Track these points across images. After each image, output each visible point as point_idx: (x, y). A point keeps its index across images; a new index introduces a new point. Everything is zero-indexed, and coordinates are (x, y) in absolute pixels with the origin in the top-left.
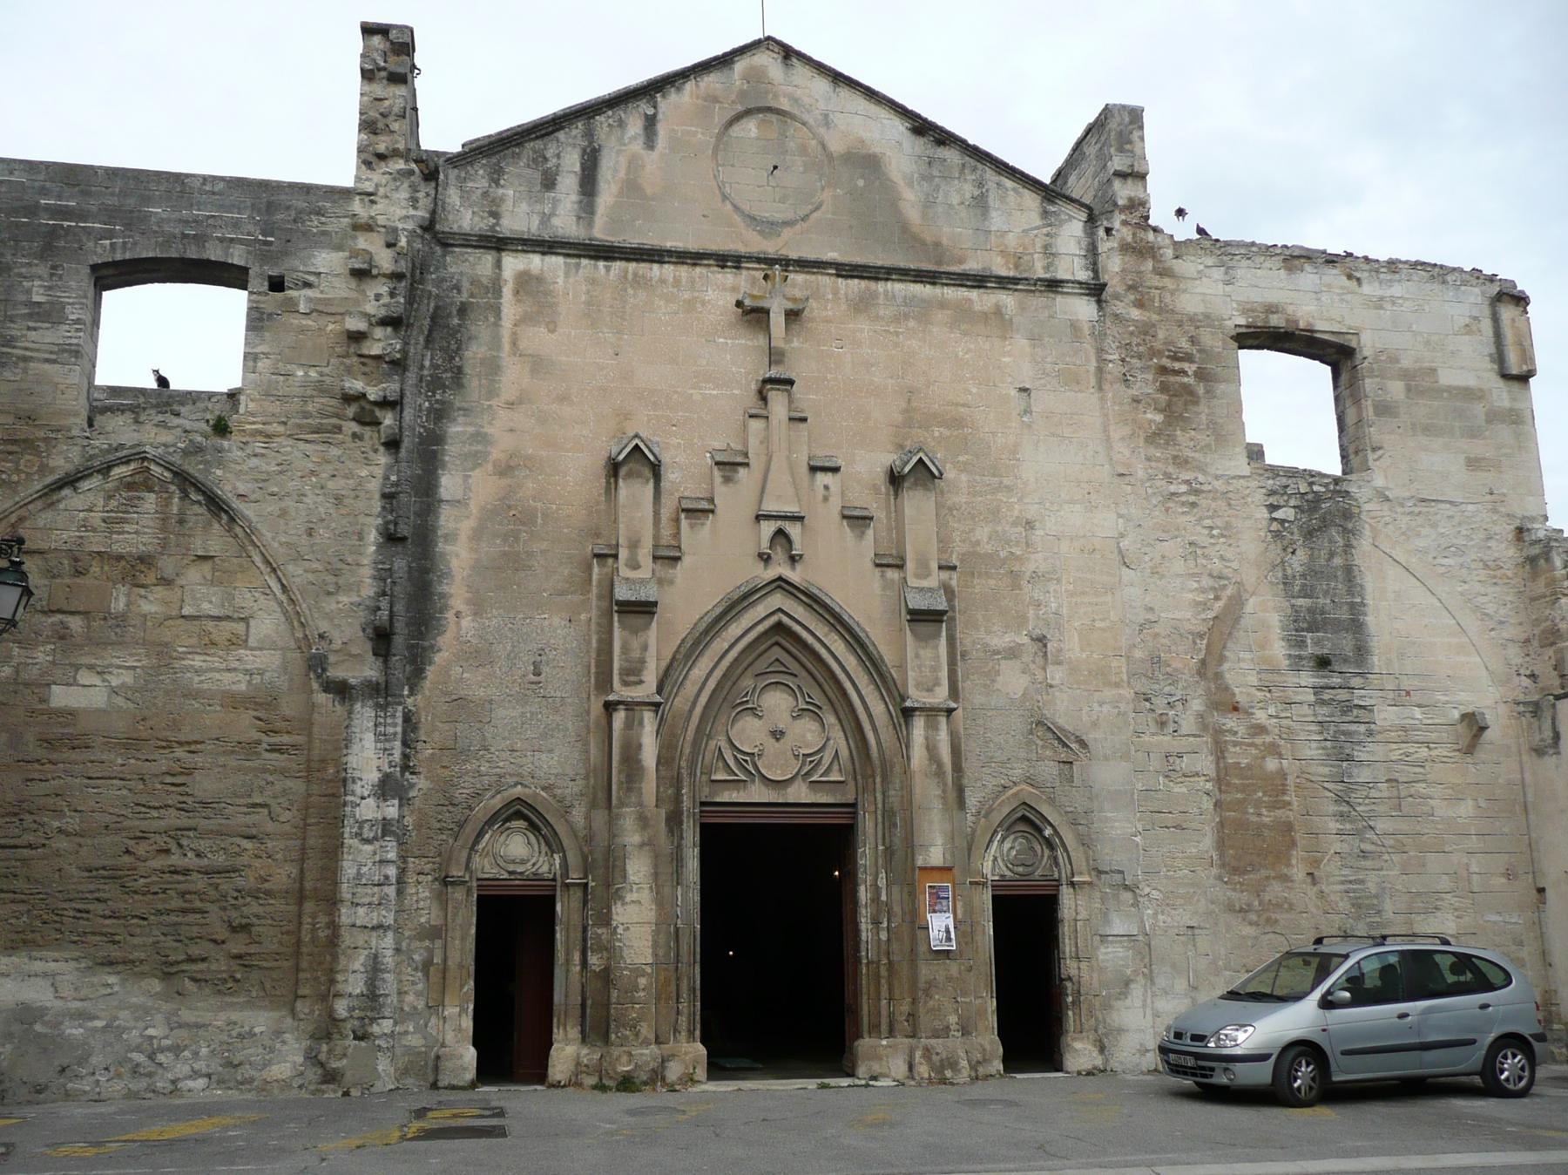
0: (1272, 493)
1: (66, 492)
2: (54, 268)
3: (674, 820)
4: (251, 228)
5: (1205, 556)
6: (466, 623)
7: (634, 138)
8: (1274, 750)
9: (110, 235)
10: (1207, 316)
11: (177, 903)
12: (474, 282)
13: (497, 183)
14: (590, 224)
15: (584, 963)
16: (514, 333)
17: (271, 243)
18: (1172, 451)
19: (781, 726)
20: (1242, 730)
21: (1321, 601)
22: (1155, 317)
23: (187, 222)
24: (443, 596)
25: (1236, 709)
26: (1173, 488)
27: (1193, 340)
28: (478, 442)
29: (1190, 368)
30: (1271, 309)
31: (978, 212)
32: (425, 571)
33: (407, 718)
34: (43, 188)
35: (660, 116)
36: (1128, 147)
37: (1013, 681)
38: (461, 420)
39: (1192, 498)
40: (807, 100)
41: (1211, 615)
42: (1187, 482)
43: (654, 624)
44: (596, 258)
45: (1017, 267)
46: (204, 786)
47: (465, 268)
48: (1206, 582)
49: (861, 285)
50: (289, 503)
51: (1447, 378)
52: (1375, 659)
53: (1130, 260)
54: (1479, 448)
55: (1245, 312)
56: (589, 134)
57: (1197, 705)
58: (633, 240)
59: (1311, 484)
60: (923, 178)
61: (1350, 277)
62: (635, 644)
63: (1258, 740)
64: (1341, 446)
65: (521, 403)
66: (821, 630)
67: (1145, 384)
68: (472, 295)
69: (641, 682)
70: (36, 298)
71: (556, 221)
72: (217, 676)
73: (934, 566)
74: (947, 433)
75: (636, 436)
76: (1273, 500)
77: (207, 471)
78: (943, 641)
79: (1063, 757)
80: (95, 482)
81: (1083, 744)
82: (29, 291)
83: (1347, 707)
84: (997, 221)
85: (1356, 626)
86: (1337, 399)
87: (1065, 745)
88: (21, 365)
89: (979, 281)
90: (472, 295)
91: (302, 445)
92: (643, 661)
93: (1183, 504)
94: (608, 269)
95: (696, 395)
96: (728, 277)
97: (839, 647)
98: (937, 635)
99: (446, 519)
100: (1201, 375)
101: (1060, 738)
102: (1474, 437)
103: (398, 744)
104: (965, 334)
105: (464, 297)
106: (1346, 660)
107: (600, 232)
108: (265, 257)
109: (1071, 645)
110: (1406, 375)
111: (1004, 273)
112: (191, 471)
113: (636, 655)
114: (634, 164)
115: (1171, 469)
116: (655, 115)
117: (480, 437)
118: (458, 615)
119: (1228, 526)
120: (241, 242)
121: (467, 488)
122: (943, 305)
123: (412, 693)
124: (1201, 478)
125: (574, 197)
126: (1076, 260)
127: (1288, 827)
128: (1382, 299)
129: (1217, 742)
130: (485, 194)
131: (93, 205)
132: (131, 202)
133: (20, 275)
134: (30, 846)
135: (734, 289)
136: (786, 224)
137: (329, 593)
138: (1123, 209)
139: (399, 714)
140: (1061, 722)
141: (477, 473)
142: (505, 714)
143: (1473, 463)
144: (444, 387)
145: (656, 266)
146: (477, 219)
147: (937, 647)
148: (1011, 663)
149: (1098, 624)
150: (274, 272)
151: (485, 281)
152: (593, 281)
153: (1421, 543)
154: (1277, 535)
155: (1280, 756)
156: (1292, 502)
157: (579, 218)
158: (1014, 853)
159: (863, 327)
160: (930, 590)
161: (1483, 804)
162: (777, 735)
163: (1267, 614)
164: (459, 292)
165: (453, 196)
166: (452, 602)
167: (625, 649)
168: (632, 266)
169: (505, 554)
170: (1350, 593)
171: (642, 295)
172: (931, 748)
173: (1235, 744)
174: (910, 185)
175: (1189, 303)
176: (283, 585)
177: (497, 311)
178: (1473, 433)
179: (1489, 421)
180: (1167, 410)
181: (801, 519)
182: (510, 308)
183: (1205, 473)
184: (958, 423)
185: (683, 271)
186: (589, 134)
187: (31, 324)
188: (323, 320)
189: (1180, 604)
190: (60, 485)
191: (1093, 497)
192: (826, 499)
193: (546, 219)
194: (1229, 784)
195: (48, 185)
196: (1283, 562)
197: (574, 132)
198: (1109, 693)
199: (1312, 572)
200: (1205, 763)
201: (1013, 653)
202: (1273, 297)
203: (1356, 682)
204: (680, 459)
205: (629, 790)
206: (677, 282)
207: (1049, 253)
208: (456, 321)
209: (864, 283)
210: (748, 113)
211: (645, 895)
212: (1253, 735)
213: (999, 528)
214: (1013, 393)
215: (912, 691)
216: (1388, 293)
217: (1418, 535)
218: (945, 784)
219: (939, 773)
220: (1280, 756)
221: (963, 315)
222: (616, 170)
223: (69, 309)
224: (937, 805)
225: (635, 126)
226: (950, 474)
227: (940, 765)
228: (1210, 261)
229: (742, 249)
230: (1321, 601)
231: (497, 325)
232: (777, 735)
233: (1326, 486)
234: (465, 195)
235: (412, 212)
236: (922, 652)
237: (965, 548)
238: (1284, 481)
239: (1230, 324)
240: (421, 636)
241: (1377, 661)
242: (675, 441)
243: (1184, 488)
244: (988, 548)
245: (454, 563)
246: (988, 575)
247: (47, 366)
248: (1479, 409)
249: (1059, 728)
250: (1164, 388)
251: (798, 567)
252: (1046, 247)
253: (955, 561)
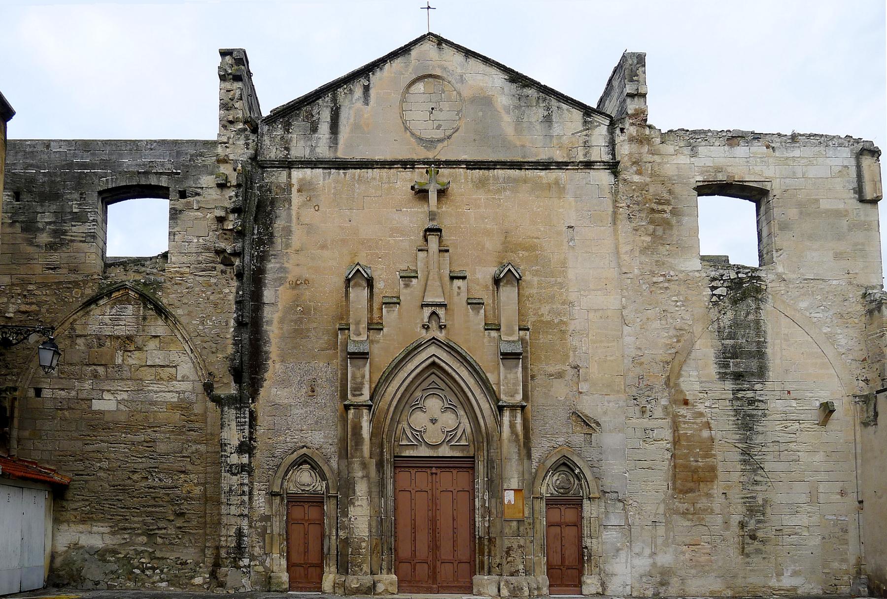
0: (714, 279)
1: (93, 306)
3: (380, 465)
5: (673, 318)
6: (277, 366)
11: (152, 502)
13: (288, 132)
14: (336, 150)
15: (337, 535)
18: (656, 257)
19: (435, 416)
20: (689, 415)
24: (266, 353)
26: (655, 279)
27: (670, 192)
28: (282, 272)
29: (668, 208)
32: (258, 340)
33: (251, 413)
35: (371, 86)
38: (273, 261)
39: (666, 285)
41: (673, 351)
42: (664, 275)
43: (368, 364)
46: (162, 447)
48: (672, 332)
49: (477, 173)
51: (825, 205)
52: (771, 373)
55: (701, 173)
59: (737, 273)
63: (698, 421)
65: (302, 250)
66: (456, 365)
69: (362, 394)
71: (318, 150)
72: (164, 394)
74: (527, 254)
75: (358, 264)
76: (714, 284)
77: (155, 293)
78: (520, 369)
79: (586, 431)
81: (598, 424)
83: (751, 402)
85: (760, 354)
87: (587, 425)
89: (546, 165)
91: (198, 278)
92: (362, 383)
93: (661, 288)
97: (464, 373)
98: (517, 366)
99: (267, 313)
102: (839, 239)
103: (247, 427)
106: (752, 374)
107: (342, 154)
109: (594, 371)
113: (359, 380)
115: (655, 268)
117: (283, 269)
119: (686, 299)
121: (277, 297)
123: (253, 402)
125: (328, 136)
130: (282, 138)
134: (88, 475)
135: (411, 180)
137: (213, 353)
139: (247, 412)
140: (587, 412)
141: (281, 288)
142: (298, 411)
144: (264, 244)
146: (278, 152)
147: (516, 373)
154: (715, 304)
158: (558, 482)
159: (481, 196)
160: (514, 342)
162: (434, 421)
163: (706, 352)
165: (267, 140)
166: (271, 355)
167: (354, 377)
169: (295, 330)
172: (512, 426)
173: (685, 423)
175: (669, 170)
180: (653, 234)
181: (445, 306)
182: (296, 198)
184: (531, 248)
186: (334, 100)
192: (459, 294)
193: (313, 149)
196: (718, 319)
197: (327, 99)
200: (668, 434)
201: (560, 375)
205: (356, 449)
206: (381, 178)
207: (587, 145)
209: (481, 172)
211: (365, 503)
212: (695, 418)
213: (555, 307)
215: (503, 397)
218: (520, 446)
219: (517, 439)
222: (348, 119)
224: (515, 457)
225: (358, 91)
226: (527, 277)
227: (517, 436)
229: (415, 157)
232: (434, 421)
233: (746, 273)
234: (272, 139)
236: (508, 376)
239: (693, 181)
240: (257, 373)
241: (771, 374)
243: (661, 279)
245: (271, 336)
248: (844, 223)
249: (586, 416)
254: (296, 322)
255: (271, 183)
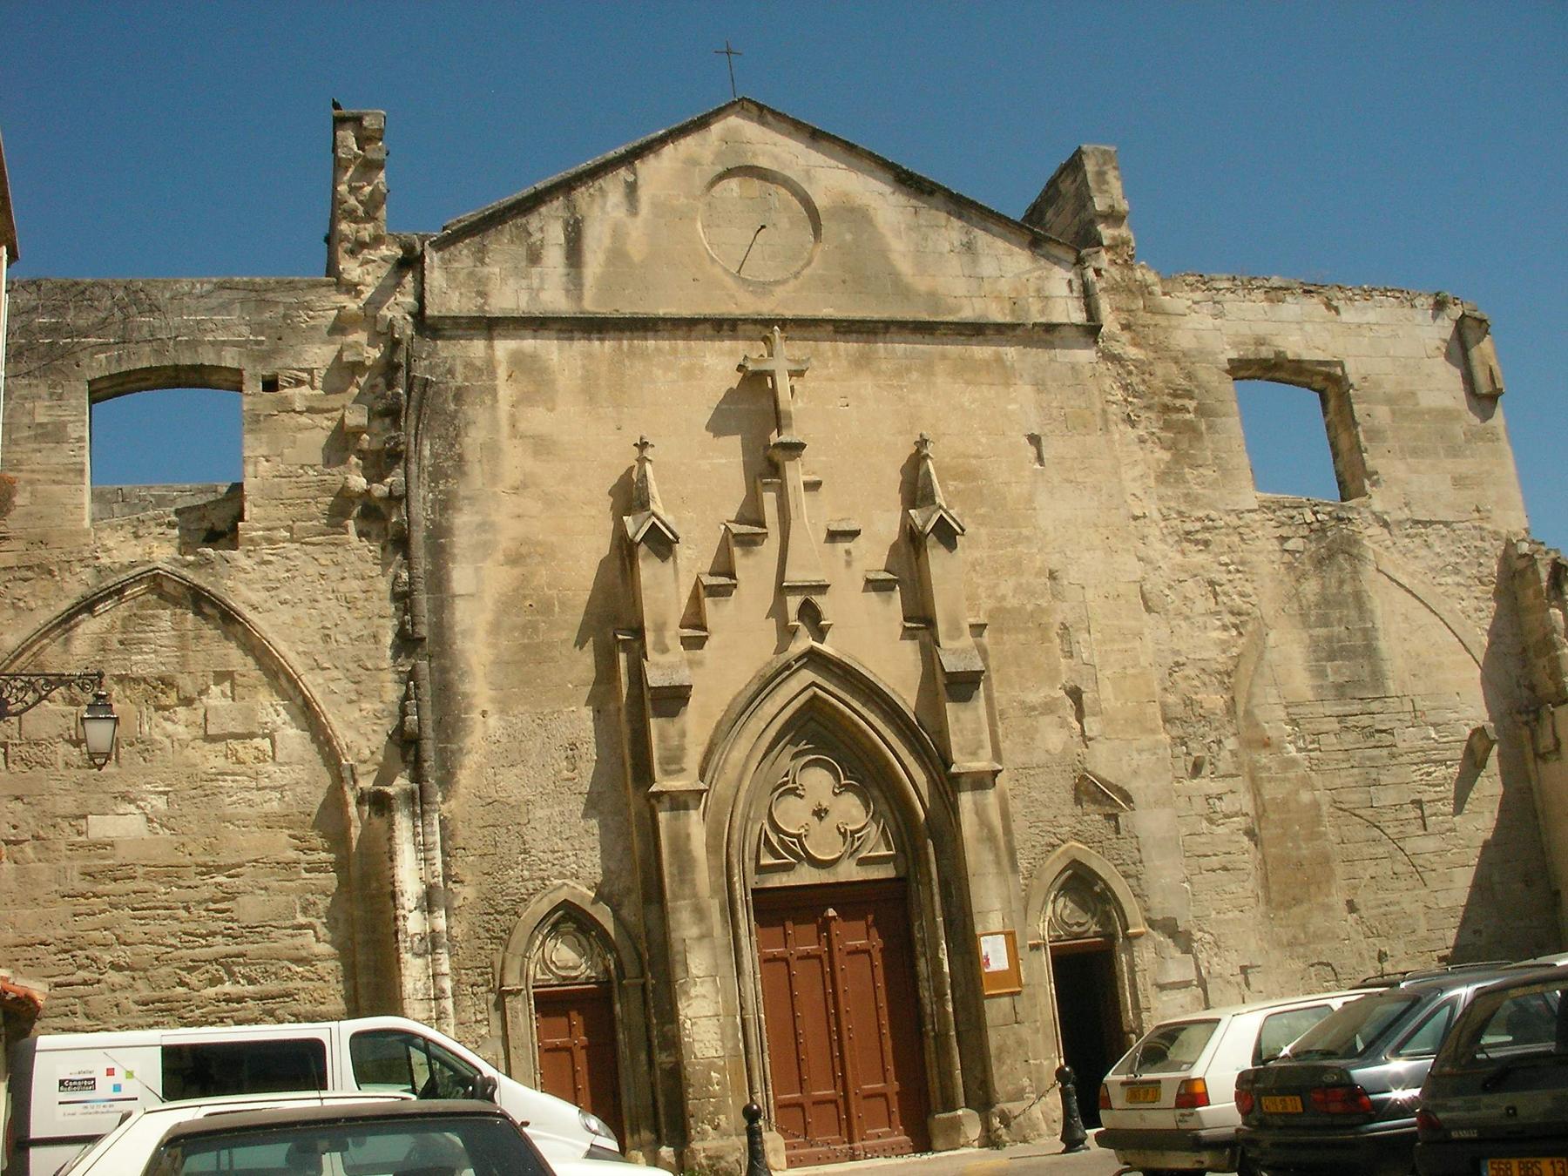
12: (469, 365)
13: (483, 263)
16: (512, 415)
22: (1152, 355)
29: (1191, 404)
38: (466, 509)
42: (1199, 519)
45: (1013, 311)
58: (627, 310)
67: (1150, 423)
90: (466, 379)
104: (968, 383)
105: (459, 380)
107: (592, 304)
111: (1000, 319)
124: (1213, 514)
130: (471, 274)
136: (777, 283)
144: (447, 476)
146: (464, 300)
151: (478, 363)
152: (589, 356)
159: (865, 384)
165: (435, 277)
169: (525, 647)
174: (898, 235)
177: (493, 391)
182: (506, 392)
183: (1216, 510)
198: (1145, 740)
208: (452, 407)
221: (965, 369)
231: (494, 407)
244: (1012, 602)
252: (1038, 290)
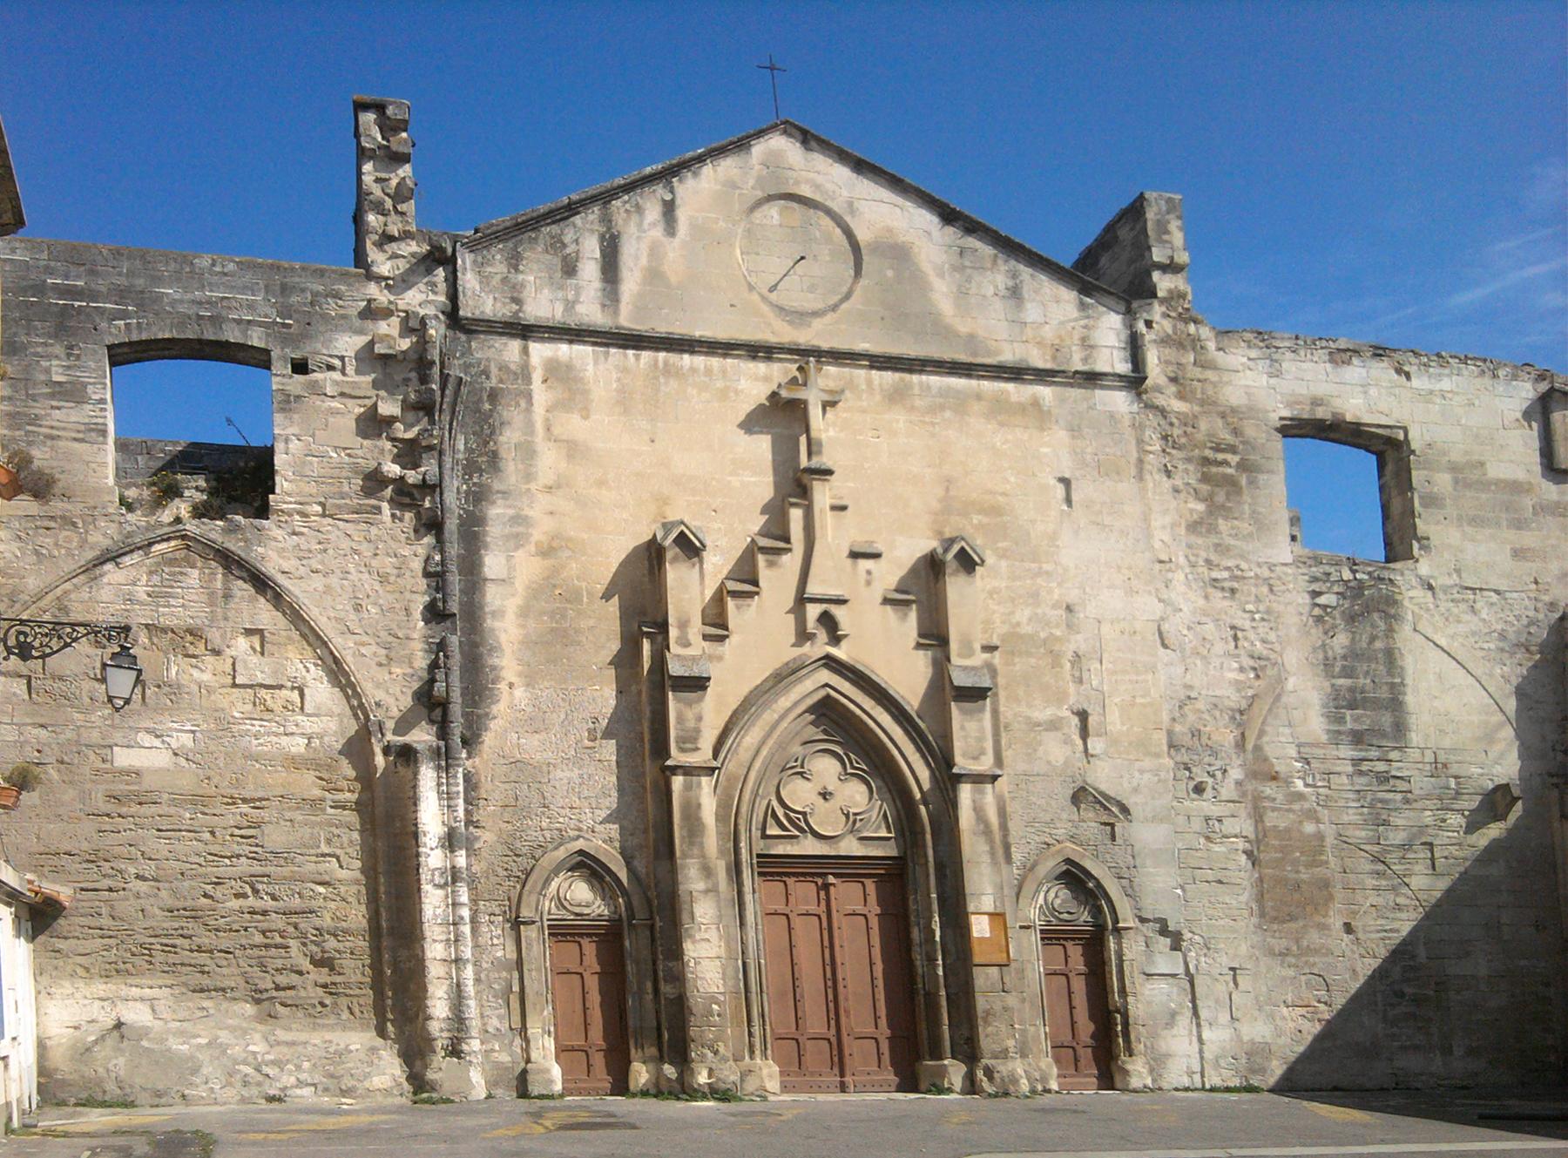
0: (1315, 579)
1: (109, 566)
2: (71, 347)
4: (269, 310)
6: (519, 692)
7: (654, 225)
8: (1312, 815)
9: (124, 315)
10: (1251, 409)
12: (503, 368)
13: (517, 270)
14: (616, 312)
15: (656, 990)
16: (547, 420)
17: (289, 326)
19: (830, 788)
20: (1280, 797)
21: (1362, 681)
22: (1197, 408)
23: (200, 303)
24: (494, 668)
25: (1274, 778)
26: (1215, 574)
27: (1236, 432)
29: (1233, 459)
30: (1316, 402)
31: (1012, 302)
32: (475, 645)
34: (47, 267)
35: (678, 202)
36: (1165, 237)
37: (1058, 751)
38: (499, 502)
40: (829, 186)
41: (1250, 693)
42: (1228, 569)
44: (625, 347)
45: (1054, 358)
47: (490, 353)
50: (334, 581)
51: (1496, 471)
52: (1413, 735)
53: (1171, 353)
54: (1529, 539)
55: (1289, 405)
56: (606, 220)
57: (1236, 774)
58: (662, 328)
60: (954, 268)
61: (1399, 371)
62: (690, 714)
63: (1296, 807)
64: (1385, 534)
65: (559, 487)
66: (868, 703)
67: (1188, 475)
68: (501, 381)
69: (697, 749)
70: (56, 378)
71: (581, 309)
73: (977, 646)
74: (985, 520)
76: (1316, 587)
77: (248, 548)
78: (987, 715)
79: (1105, 819)
80: (136, 557)
81: (1125, 810)
82: (48, 371)
83: (1383, 778)
84: (1032, 312)
85: (1395, 704)
86: (1381, 489)
87: (1106, 808)
88: (49, 443)
89: (1016, 373)
90: (501, 381)
94: (637, 358)
95: (735, 482)
96: (761, 367)
97: (885, 719)
98: (982, 710)
99: (493, 596)
100: (1243, 466)
101: (1102, 802)
102: (1519, 528)
104: (1002, 424)
105: (494, 382)
106: (1384, 735)
107: (626, 320)
108: (286, 340)
110: (1454, 468)
111: (1041, 365)
112: (233, 548)
114: (655, 251)
115: (1213, 557)
116: (673, 201)
117: (519, 519)
118: (511, 685)
119: (1268, 611)
120: (260, 324)
121: (511, 568)
122: (979, 397)
123: (469, 756)
124: (1244, 565)
126: (1115, 352)
127: (1325, 884)
128: (1431, 392)
129: (1256, 808)
130: (505, 280)
131: (101, 285)
132: (140, 282)
133: (36, 354)
135: (767, 379)
136: (816, 314)
138: (1163, 301)
140: (1103, 787)
141: (520, 554)
142: (562, 775)
143: (1518, 554)
144: (481, 471)
145: (686, 357)
146: (499, 305)
147: (980, 720)
148: (1052, 734)
149: (1138, 700)
150: (297, 355)
151: (513, 367)
152: (625, 370)
153: (1461, 628)
155: (1318, 821)
156: (1336, 589)
157: (604, 306)
159: (899, 419)
160: (973, 668)
161: (1515, 864)
164: (488, 378)
165: (469, 280)
166: (503, 674)
168: (662, 355)
169: (552, 630)
170: (1390, 673)
171: (674, 384)
174: (941, 275)
176: (335, 657)
177: (529, 396)
178: (1519, 524)
179: (1535, 513)
180: (1208, 499)
181: (844, 602)
182: (541, 395)
183: (1247, 561)
184: (995, 511)
185: (715, 362)
186: (606, 220)
187: (54, 403)
188: (350, 402)
189: (1223, 679)
190: (101, 561)
191: (1134, 582)
192: (868, 583)
193: (570, 306)
194: (1267, 845)
195: (52, 264)
196: (1324, 645)
197: (591, 217)
199: (1353, 654)
201: (1054, 725)
202: (1321, 389)
203: (1394, 755)
204: (723, 542)
207: (1087, 345)
208: (487, 406)
209: (897, 375)
210: (770, 198)
212: (1291, 802)
213: (1039, 611)
214: (1053, 482)
216: (1438, 387)
217: (1459, 622)
220: (1318, 821)
221: (999, 410)
222: (637, 258)
223: (90, 389)
225: (653, 212)
226: (990, 559)
228: (1254, 353)
229: (773, 339)
230: (1362, 681)
231: (529, 409)
234: (484, 280)
235: (432, 297)
236: (967, 724)
237: (1005, 629)
238: (1328, 569)
240: (475, 704)
241: (1415, 738)
242: (716, 526)
243: (1226, 574)
245: (503, 638)
246: (1029, 654)
247: (76, 445)
248: (1528, 502)
249: (1101, 793)
250: (1205, 478)
251: (844, 643)
252: (1083, 339)
253: (995, 641)
254: (552, 614)
255: (488, 360)
